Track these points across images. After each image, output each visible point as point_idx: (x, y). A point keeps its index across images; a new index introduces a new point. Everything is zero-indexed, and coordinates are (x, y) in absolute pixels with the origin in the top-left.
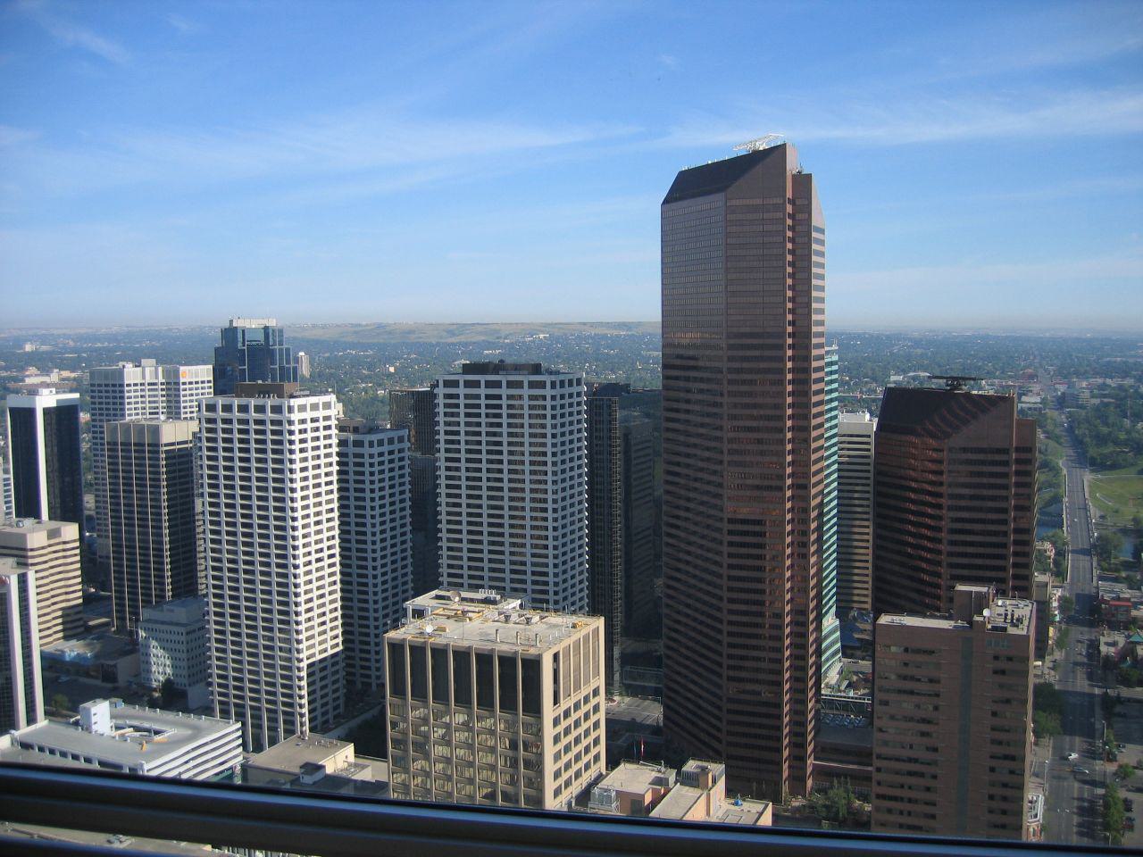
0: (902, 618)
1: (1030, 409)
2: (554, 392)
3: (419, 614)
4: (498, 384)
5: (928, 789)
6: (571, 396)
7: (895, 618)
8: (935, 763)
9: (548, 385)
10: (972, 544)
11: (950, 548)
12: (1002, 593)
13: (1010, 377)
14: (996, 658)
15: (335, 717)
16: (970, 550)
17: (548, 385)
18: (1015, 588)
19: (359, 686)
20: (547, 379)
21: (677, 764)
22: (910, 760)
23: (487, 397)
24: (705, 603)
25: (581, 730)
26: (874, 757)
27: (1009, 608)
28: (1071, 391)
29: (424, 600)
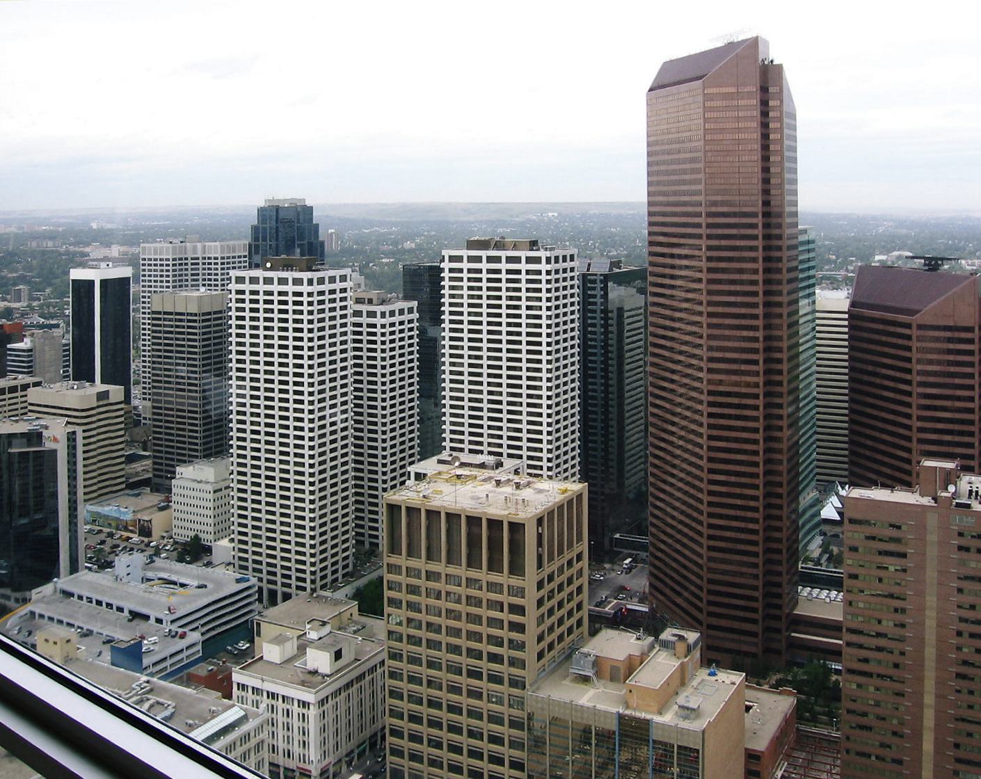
2: (549, 267)
3: (420, 477)
4: (497, 260)
5: (896, 666)
6: (565, 271)
8: (901, 640)
9: (544, 260)
10: (939, 420)
11: (919, 424)
12: (968, 469)
14: (961, 534)
15: (344, 576)
16: (940, 426)
17: (544, 260)
19: (367, 545)
20: (542, 254)
21: (655, 632)
22: (879, 635)
23: (469, 271)
24: (689, 473)
25: (564, 594)
26: (844, 630)
29: (429, 466)
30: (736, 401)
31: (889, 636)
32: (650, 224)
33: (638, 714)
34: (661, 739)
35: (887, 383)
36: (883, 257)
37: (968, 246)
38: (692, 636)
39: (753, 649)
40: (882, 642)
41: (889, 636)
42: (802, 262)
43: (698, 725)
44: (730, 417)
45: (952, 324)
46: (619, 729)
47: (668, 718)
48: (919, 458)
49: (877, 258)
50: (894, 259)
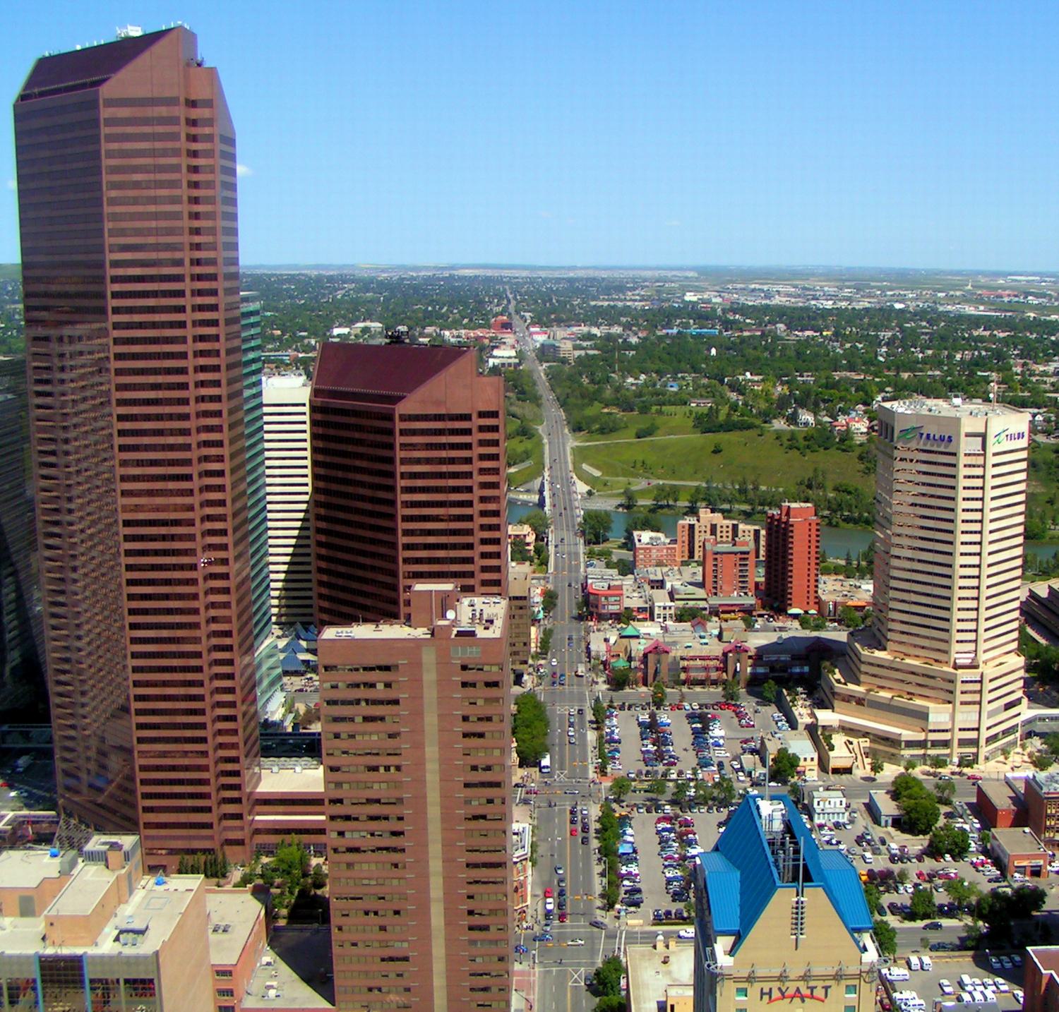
0: (348, 630)
1: (503, 365)
7: (340, 630)
8: (400, 801)
13: (481, 326)
14: (464, 668)
18: (485, 583)
27: (478, 608)
28: (551, 341)
30: (163, 530)
31: (382, 801)
32: (28, 295)
33: (66, 951)
34: (99, 976)
35: (361, 491)
36: (345, 331)
37: (452, 312)
38: (128, 841)
39: (206, 844)
40: (375, 809)
41: (382, 801)
42: (245, 340)
43: (147, 947)
44: (156, 553)
45: (443, 412)
46: (42, 975)
47: (106, 946)
48: (408, 582)
49: (336, 331)
50: (358, 331)
